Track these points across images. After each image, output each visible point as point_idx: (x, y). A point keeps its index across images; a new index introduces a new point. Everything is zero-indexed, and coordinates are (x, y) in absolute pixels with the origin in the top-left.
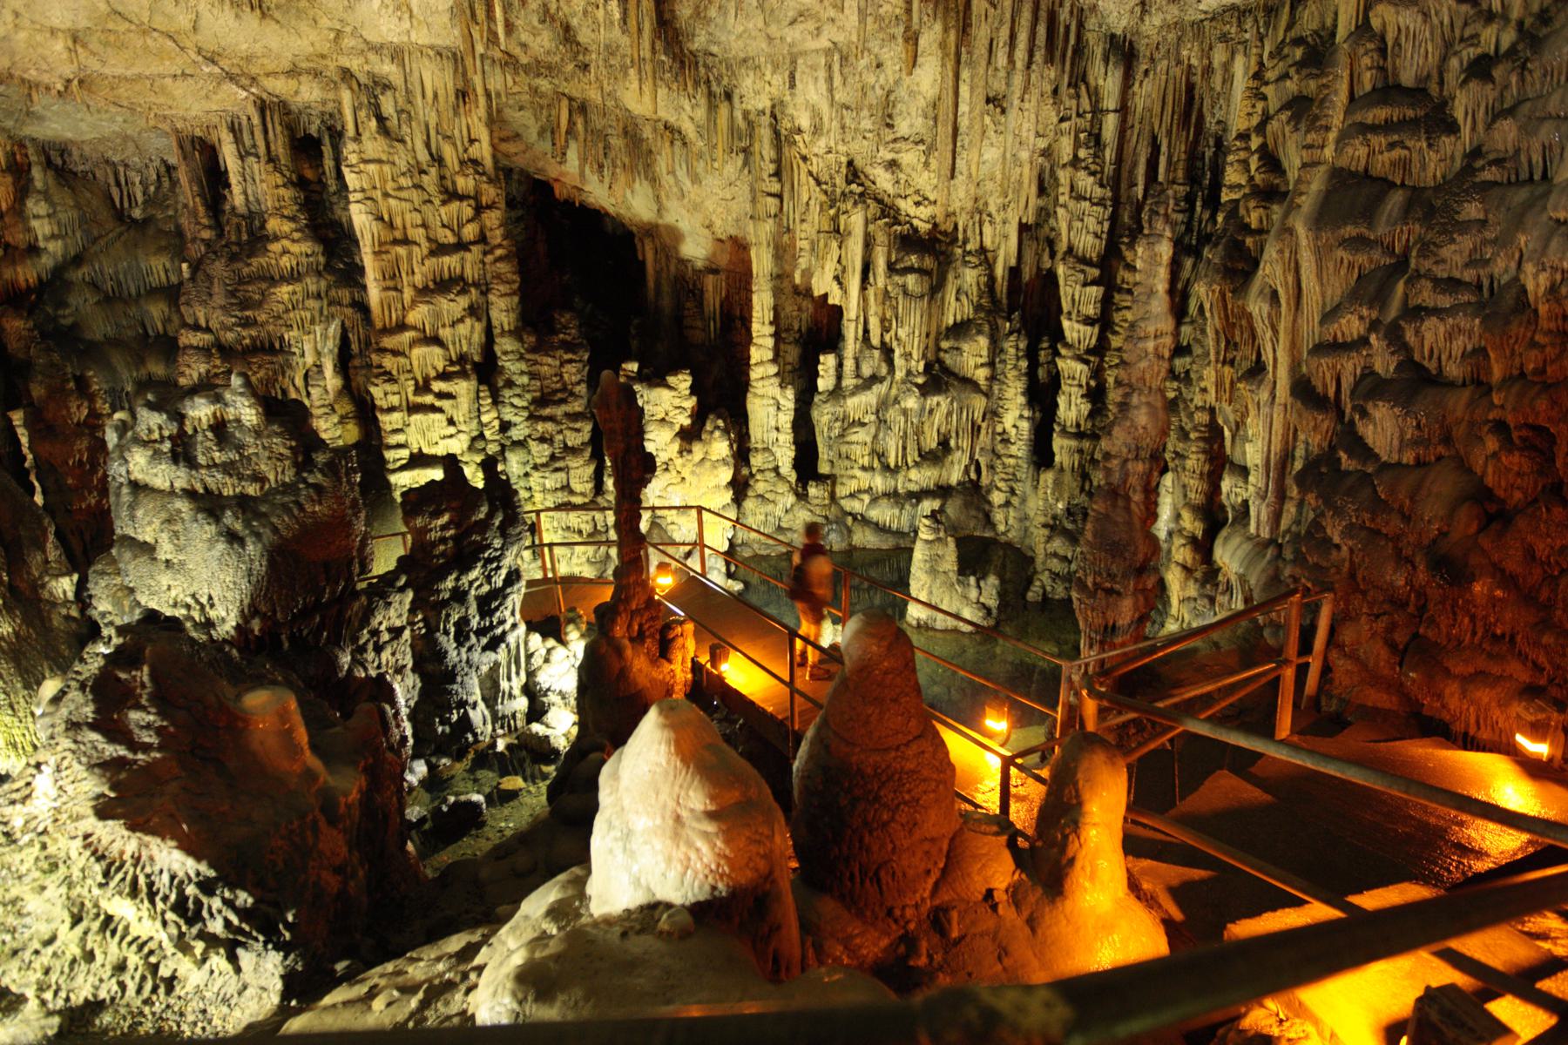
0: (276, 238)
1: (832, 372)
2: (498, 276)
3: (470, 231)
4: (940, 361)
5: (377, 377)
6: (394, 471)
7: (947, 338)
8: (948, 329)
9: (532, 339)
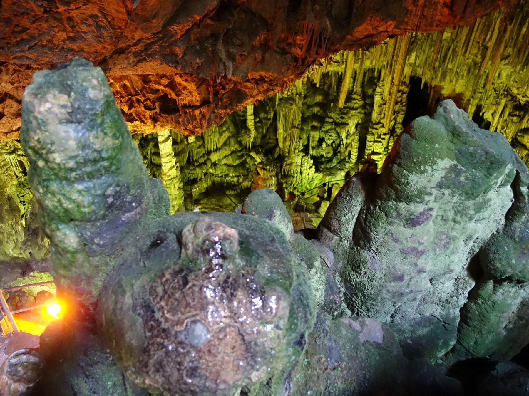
0: (355, 99)
2: (402, 110)
3: (399, 99)
4: (516, 139)
7: (520, 132)
8: (522, 130)
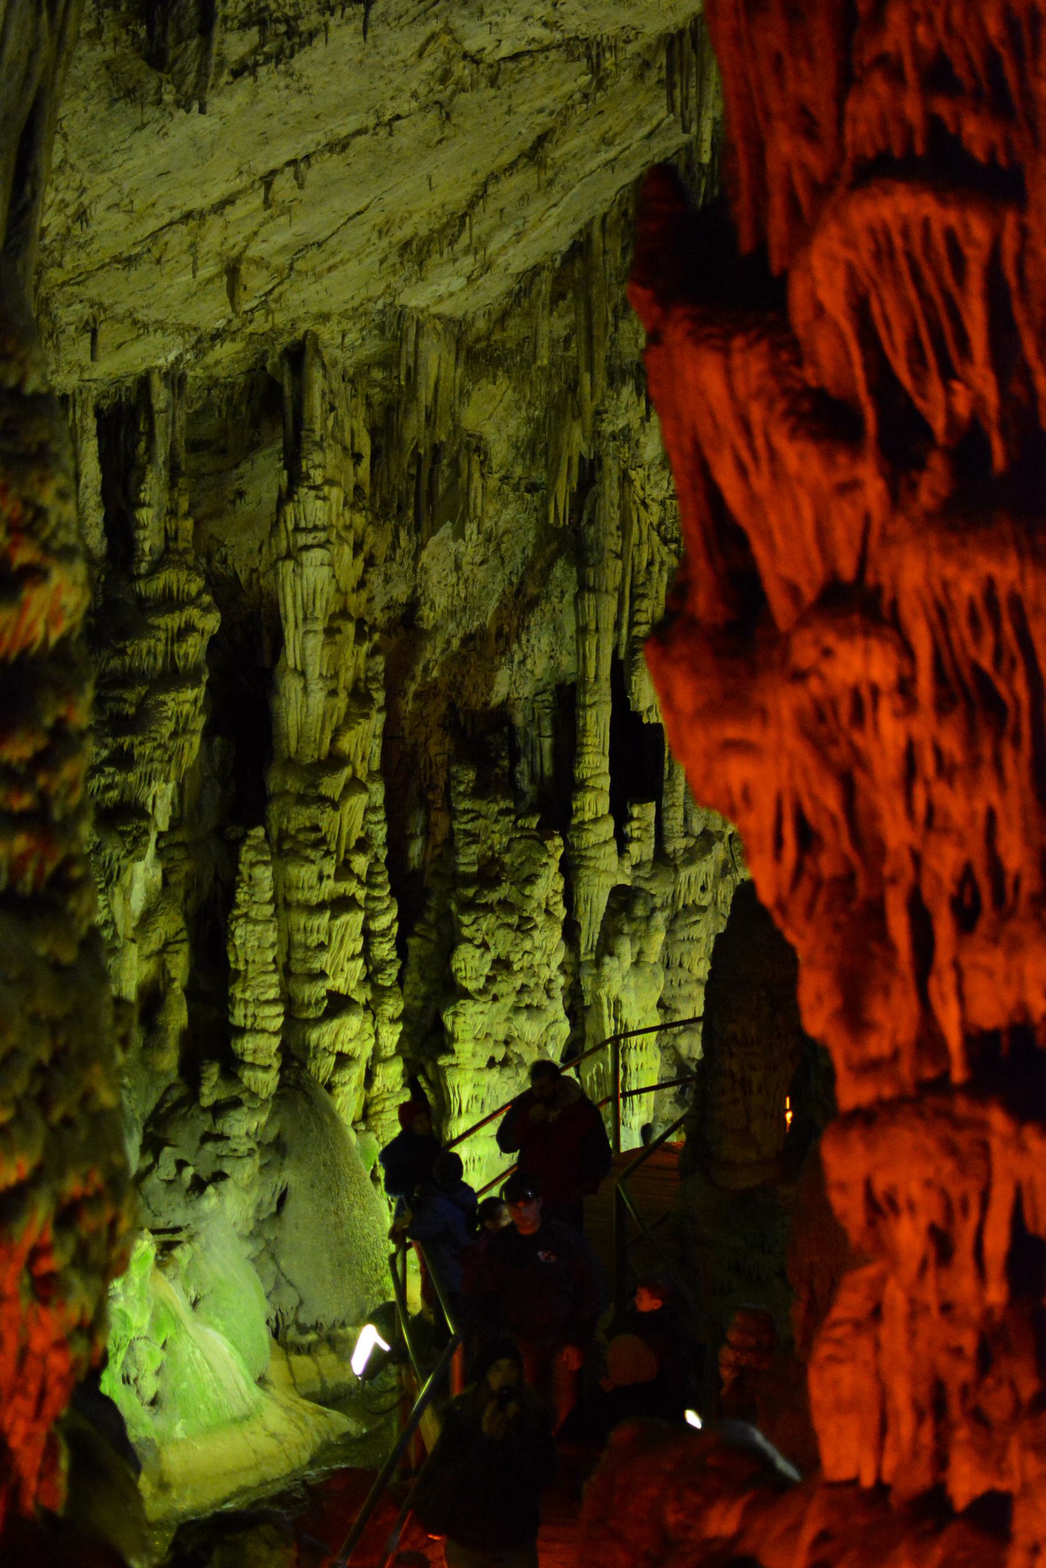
0: (171, 602)
1: (652, 829)
5: (317, 844)
6: (319, 1021)
9: (472, 775)
